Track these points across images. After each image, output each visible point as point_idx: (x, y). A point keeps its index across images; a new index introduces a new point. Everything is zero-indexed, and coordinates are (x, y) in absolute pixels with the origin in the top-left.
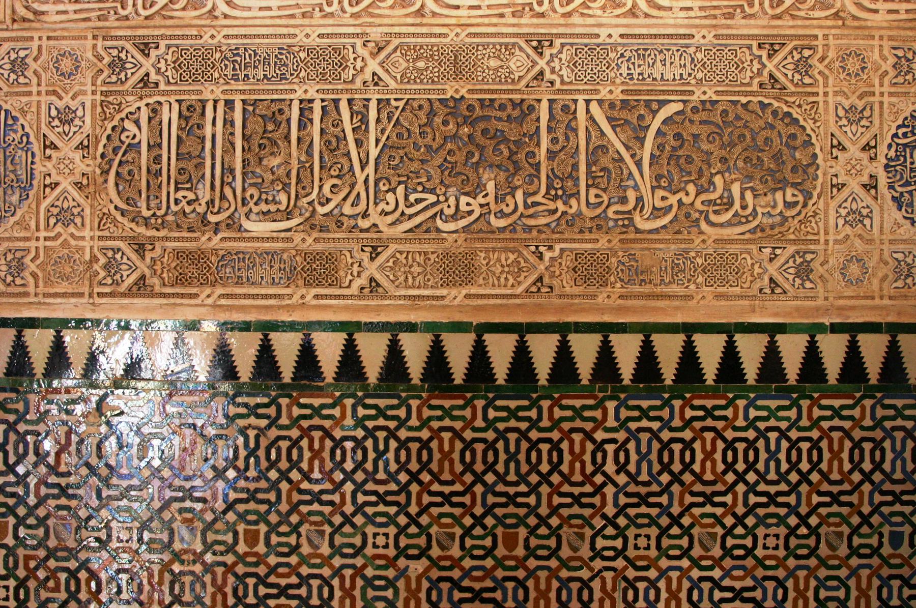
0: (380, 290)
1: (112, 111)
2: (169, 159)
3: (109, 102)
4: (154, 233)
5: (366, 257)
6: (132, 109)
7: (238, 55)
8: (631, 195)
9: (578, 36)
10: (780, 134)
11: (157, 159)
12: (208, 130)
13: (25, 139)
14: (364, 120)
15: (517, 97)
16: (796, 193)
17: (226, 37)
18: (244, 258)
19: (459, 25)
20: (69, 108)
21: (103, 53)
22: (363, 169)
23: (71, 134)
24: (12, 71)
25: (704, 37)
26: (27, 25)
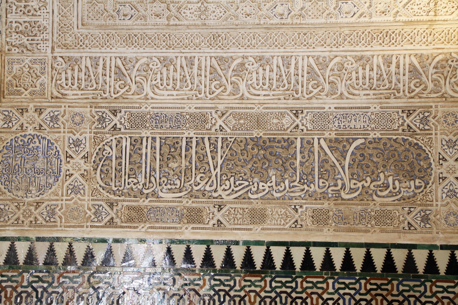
0: (222, 225)
1: (99, 141)
2: (125, 164)
3: (98, 137)
4: (118, 198)
5: (216, 210)
6: (108, 140)
7: (158, 116)
8: (340, 182)
9: (315, 108)
10: (412, 154)
11: (120, 164)
12: (144, 151)
13: (57, 153)
14: (216, 147)
15: (286, 137)
16: (420, 181)
17: (153, 108)
18: (160, 210)
19: (259, 104)
20: (79, 139)
21: (95, 114)
22: (215, 170)
23: (79, 151)
25: (375, 108)
26: (58, 100)
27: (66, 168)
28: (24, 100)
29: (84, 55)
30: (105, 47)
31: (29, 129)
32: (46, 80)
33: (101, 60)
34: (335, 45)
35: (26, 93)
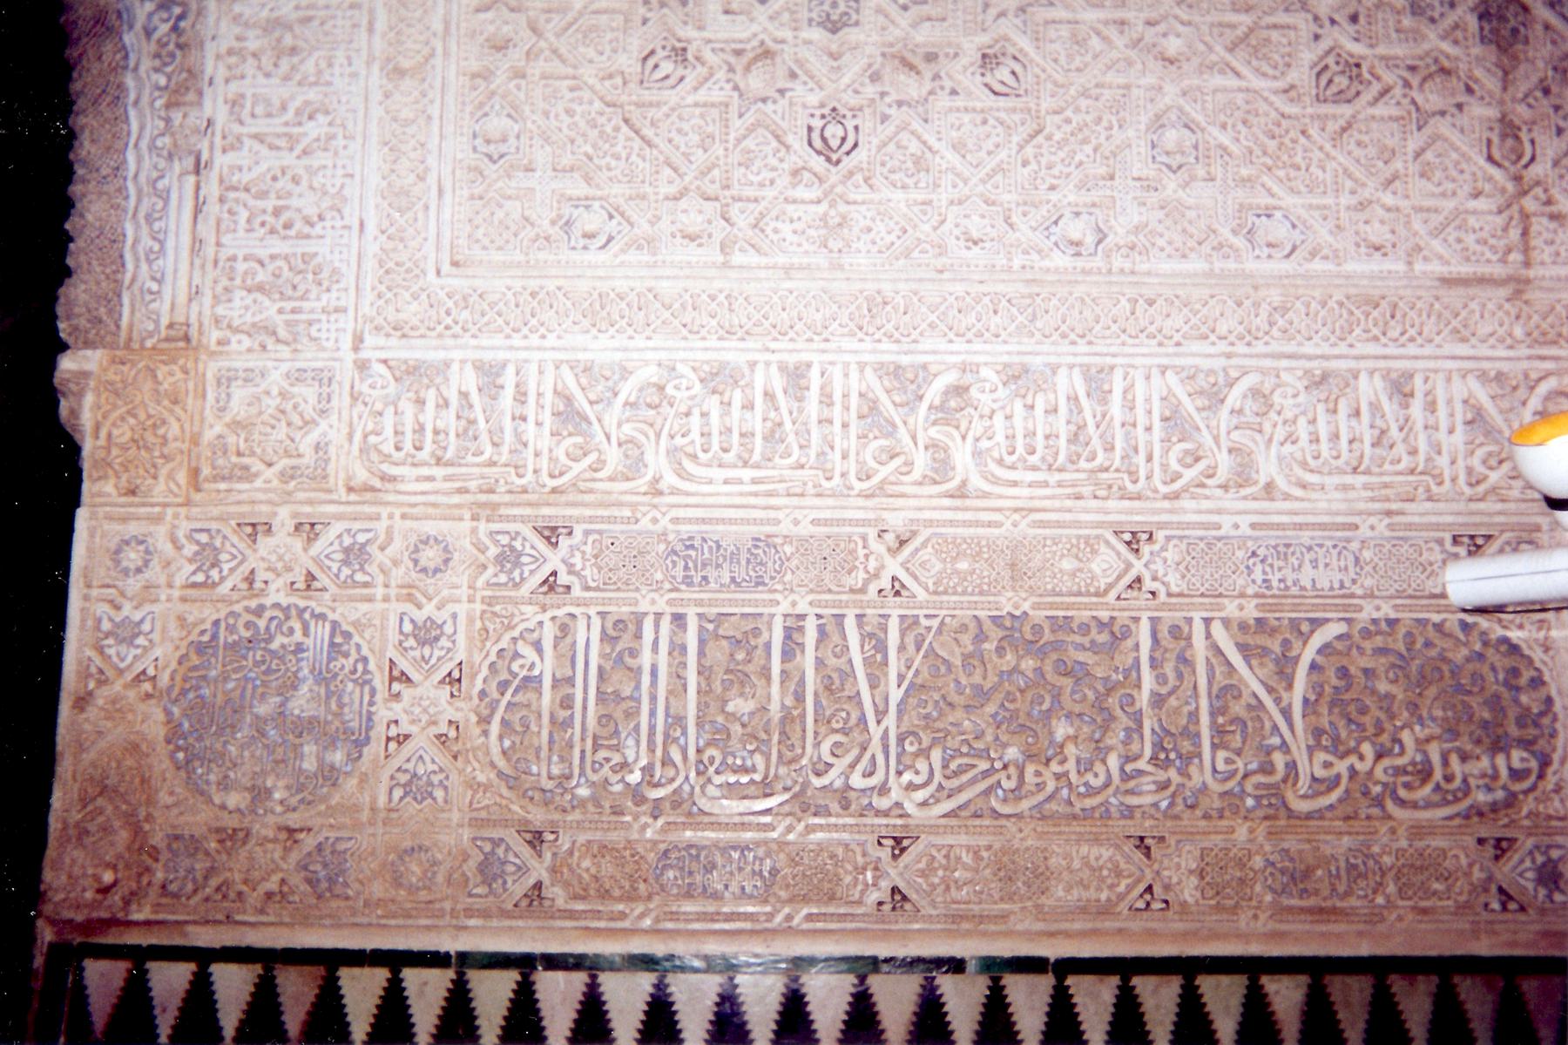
0: (908, 906)
1: (498, 626)
2: (585, 700)
3: (495, 614)
5: (885, 854)
6: (531, 625)
7: (692, 547)
8: (1279, 759)
9: (1189, 526)
10: (1493, 669)
11: (567, 703)
12: (646, 659)
13: (360, 667)
14: (881, 647)
15: (1104, 615)
16: (1525, 755)
17: (675, 520)
18: (698, 856)
19: (1016, 510)
20: (433, 622)
21: (488, 542)
22: (879, 722)
23: (433, 661)
24: (346, 562)
25: (1372, 528)
26: (368, 496)
27: (391, 716)
28: (261, 496)
29: (457, 355)
30: (525, 331)
31: (272, 587)
32: (332, 435)
33: (511, 370)
34: (1241, 338)
35: (270, 473)
